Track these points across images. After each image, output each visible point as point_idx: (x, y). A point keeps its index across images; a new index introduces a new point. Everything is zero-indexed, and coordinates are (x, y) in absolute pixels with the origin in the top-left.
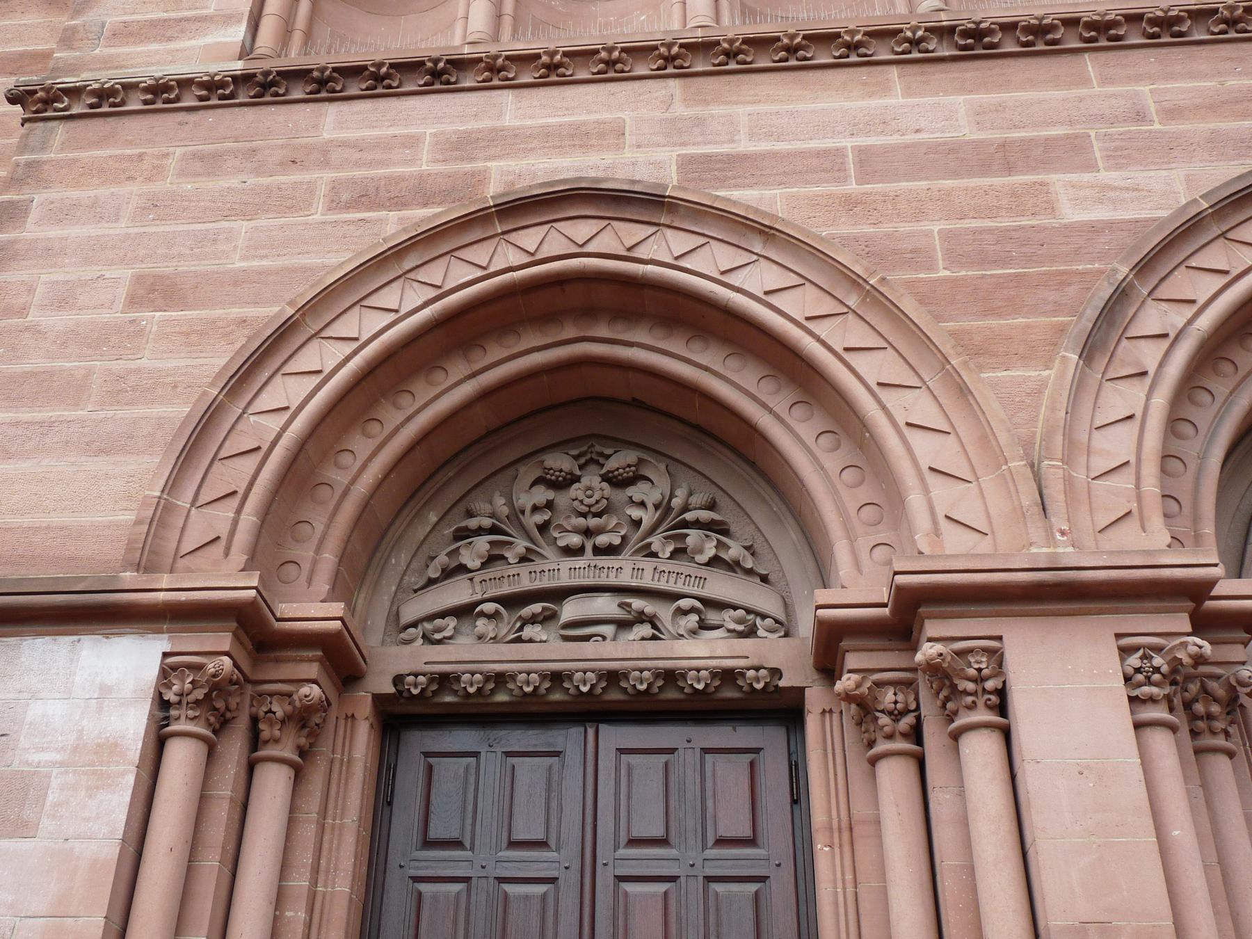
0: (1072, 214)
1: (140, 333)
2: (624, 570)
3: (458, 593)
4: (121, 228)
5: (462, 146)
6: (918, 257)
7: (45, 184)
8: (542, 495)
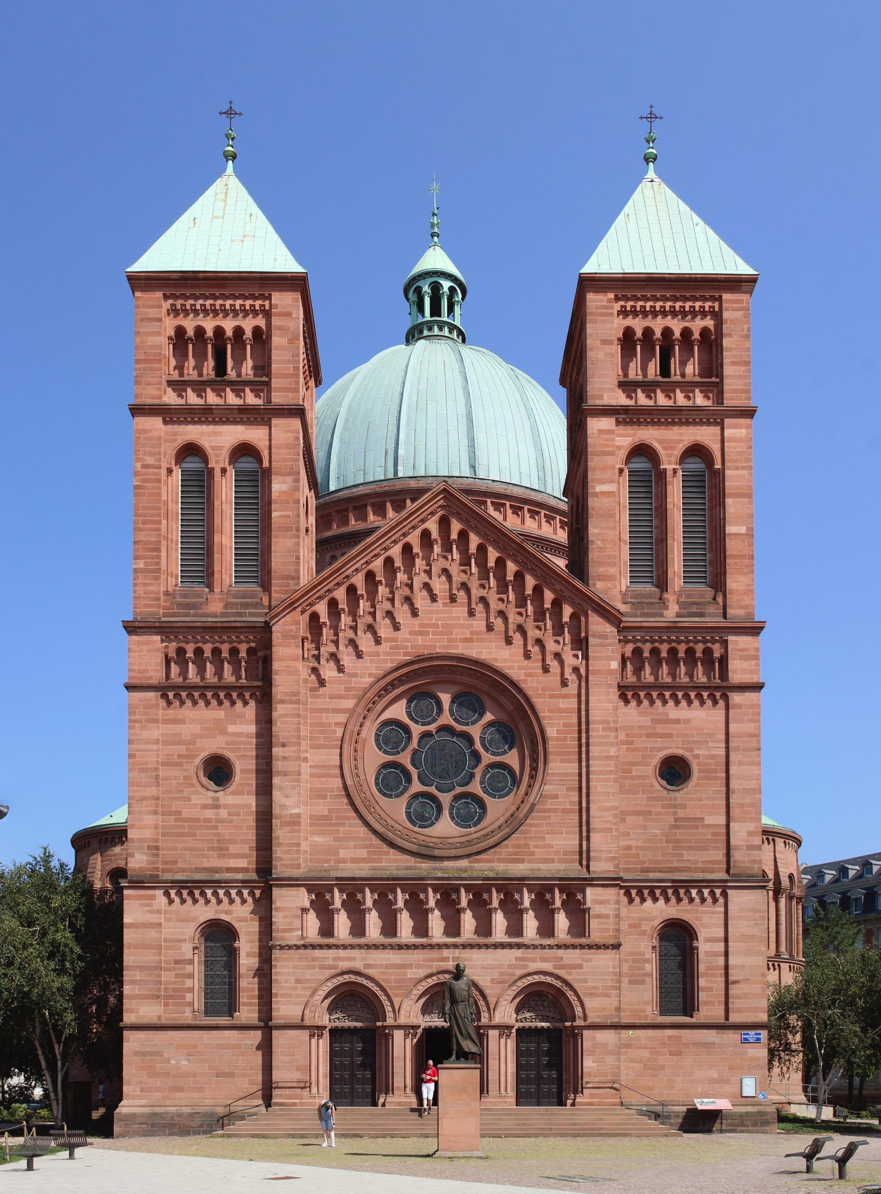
0: (409, 976)
1: (297, 988)
2: (356, 1013)
3: (337, 1016)
4: (291, 970)
5: (335, 959)
6: (390, 982)
7: (278, 961)
8: (346, 1003)
